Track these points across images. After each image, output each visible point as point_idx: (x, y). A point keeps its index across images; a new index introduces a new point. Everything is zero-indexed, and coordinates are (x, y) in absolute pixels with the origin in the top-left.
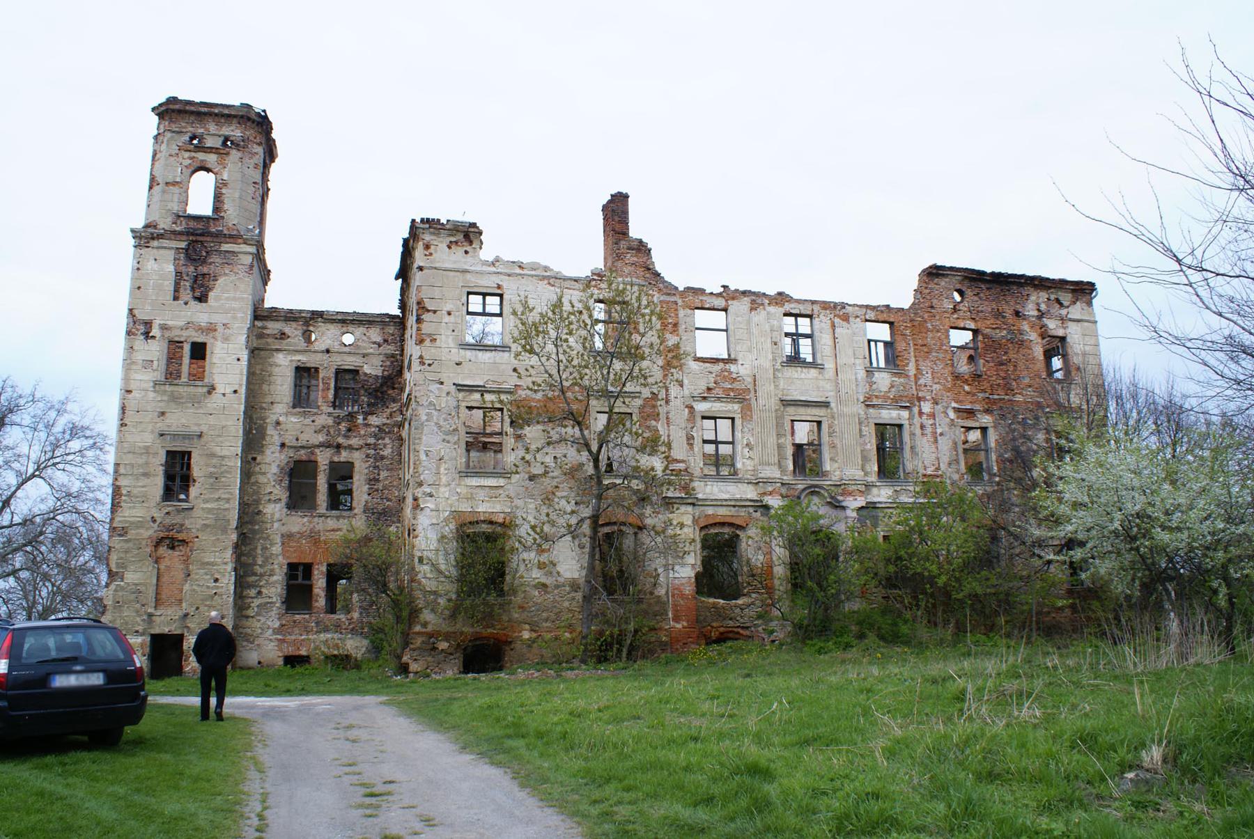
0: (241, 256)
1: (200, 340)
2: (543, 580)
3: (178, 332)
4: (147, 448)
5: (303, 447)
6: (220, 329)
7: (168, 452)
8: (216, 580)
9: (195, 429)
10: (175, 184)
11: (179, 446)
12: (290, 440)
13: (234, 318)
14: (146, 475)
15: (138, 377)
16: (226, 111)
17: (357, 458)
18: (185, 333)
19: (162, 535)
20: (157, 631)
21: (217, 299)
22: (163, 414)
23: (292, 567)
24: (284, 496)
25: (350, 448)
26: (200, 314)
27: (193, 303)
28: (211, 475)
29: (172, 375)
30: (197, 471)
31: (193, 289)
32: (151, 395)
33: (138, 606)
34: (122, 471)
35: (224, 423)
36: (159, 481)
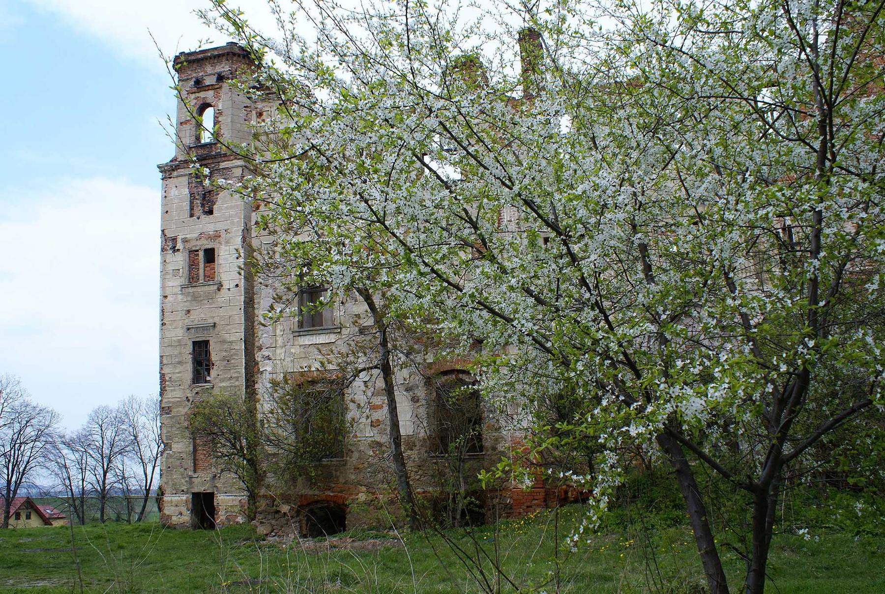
0: (234, 170)
1: (210, 247)
2: (378, 438)
3: (193, 243)
4: (179, 341)
7: (194, 342)
9: (211, 321)
13: (233, 223)
14: (180, 363)
15: (170, 284)
16: (216, 53)
18: (199, 243)
20: (196, 490)
21: (220, 209)
22: (189, 311)
26: (207, 225)
27: (203, 217)
28: (224, 359)
29: (192, 279)
30: (214, 357)
31: (203, 205)
32: (180, 297)
33: (182, 470)
34: (165, 362)
35: (230, 314)
36: (189, 367)
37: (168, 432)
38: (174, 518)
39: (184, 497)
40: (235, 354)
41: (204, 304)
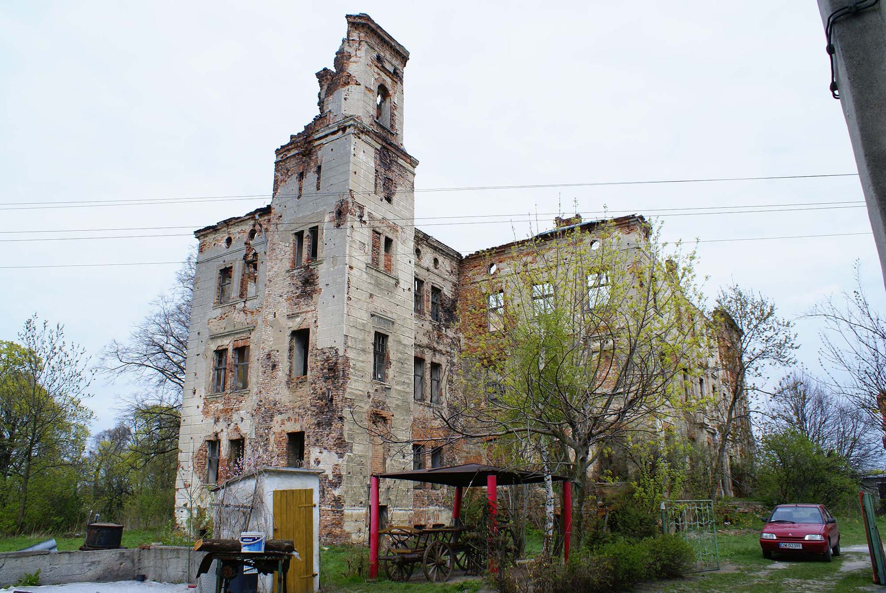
25: (440, 352)
32: (365, 276)
33: (361, 477)
37: (350, 430)
38: (354, 536)
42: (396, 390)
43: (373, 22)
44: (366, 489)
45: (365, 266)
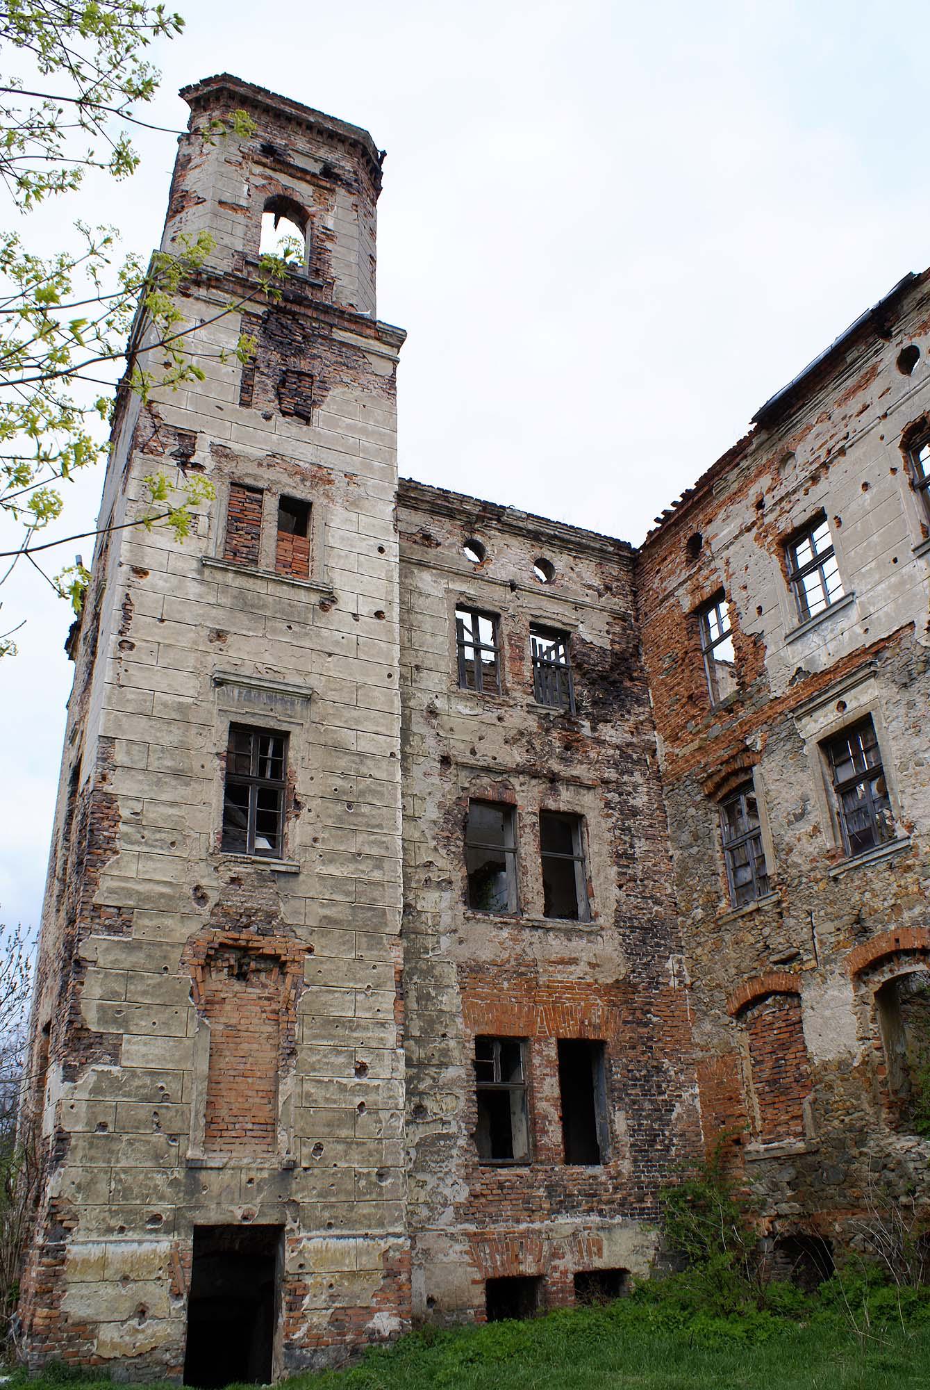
3: (253, 469)
4: (181, 708)
5: (487, 770)
6: (340, 481)
7: (234, 727)
8: (361, 1069)
10: (236, 207)
11: (260, 715)
12: (459, 751)
13: (370, 468)
14: (180, 775)
16: (329, 125)
17: (589, 804)
19: (221, 937)
20: (211, 1216)
21: (331, 422)
22: (220, 635)
23: (483, 1044)
24: (459, 875)
25: (575, 782)
27: (279, 419)
28: (336, 796)
29: (238, 556)
32: (193, 589)
33: (159, 1138)
34: (120, 756)
35: (360, 678)
36: (214, 794)
39: (164, 1245)
40: (373, 792)
41: (274, 631)
42: (321, 877)
43: (237, 81)
44: (179, 1174)
45: (195, 565)
